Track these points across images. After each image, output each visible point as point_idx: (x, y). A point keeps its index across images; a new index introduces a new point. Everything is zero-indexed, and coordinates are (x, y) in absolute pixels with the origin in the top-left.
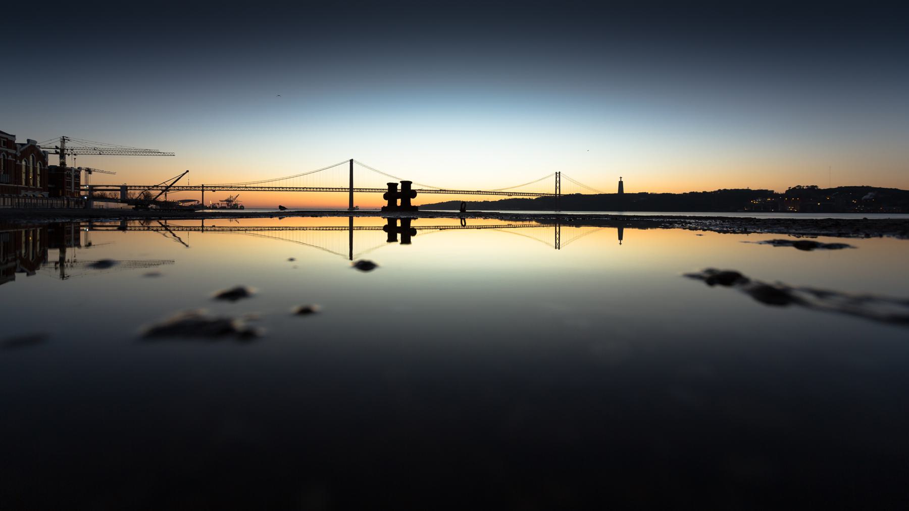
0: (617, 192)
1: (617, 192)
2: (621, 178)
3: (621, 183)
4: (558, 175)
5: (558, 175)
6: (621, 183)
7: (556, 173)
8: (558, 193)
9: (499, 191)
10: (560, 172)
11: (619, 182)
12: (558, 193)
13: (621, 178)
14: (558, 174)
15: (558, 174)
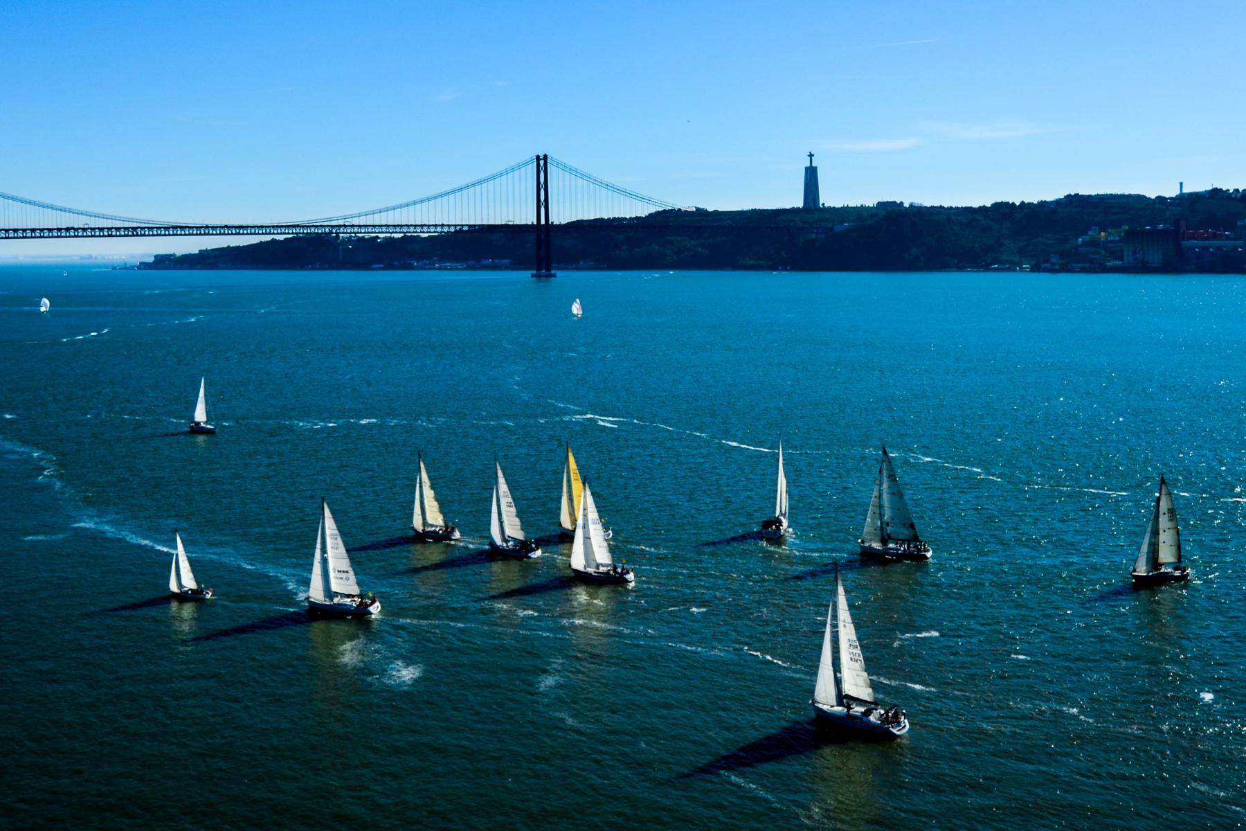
0: (800, 204)
1: (800, 204)
2: (811, 155)
3: (811, 175)
4: (542, 163)
5: (542, 163)
6: (811, 175)
7: (538, 158)
8: (543, 222)
9: (341, 223)
10: (545, 157)
11: (807, 169)
12: (543, 222)
13: (811, 155)
14: (542, 162)
15: (542, 162)
